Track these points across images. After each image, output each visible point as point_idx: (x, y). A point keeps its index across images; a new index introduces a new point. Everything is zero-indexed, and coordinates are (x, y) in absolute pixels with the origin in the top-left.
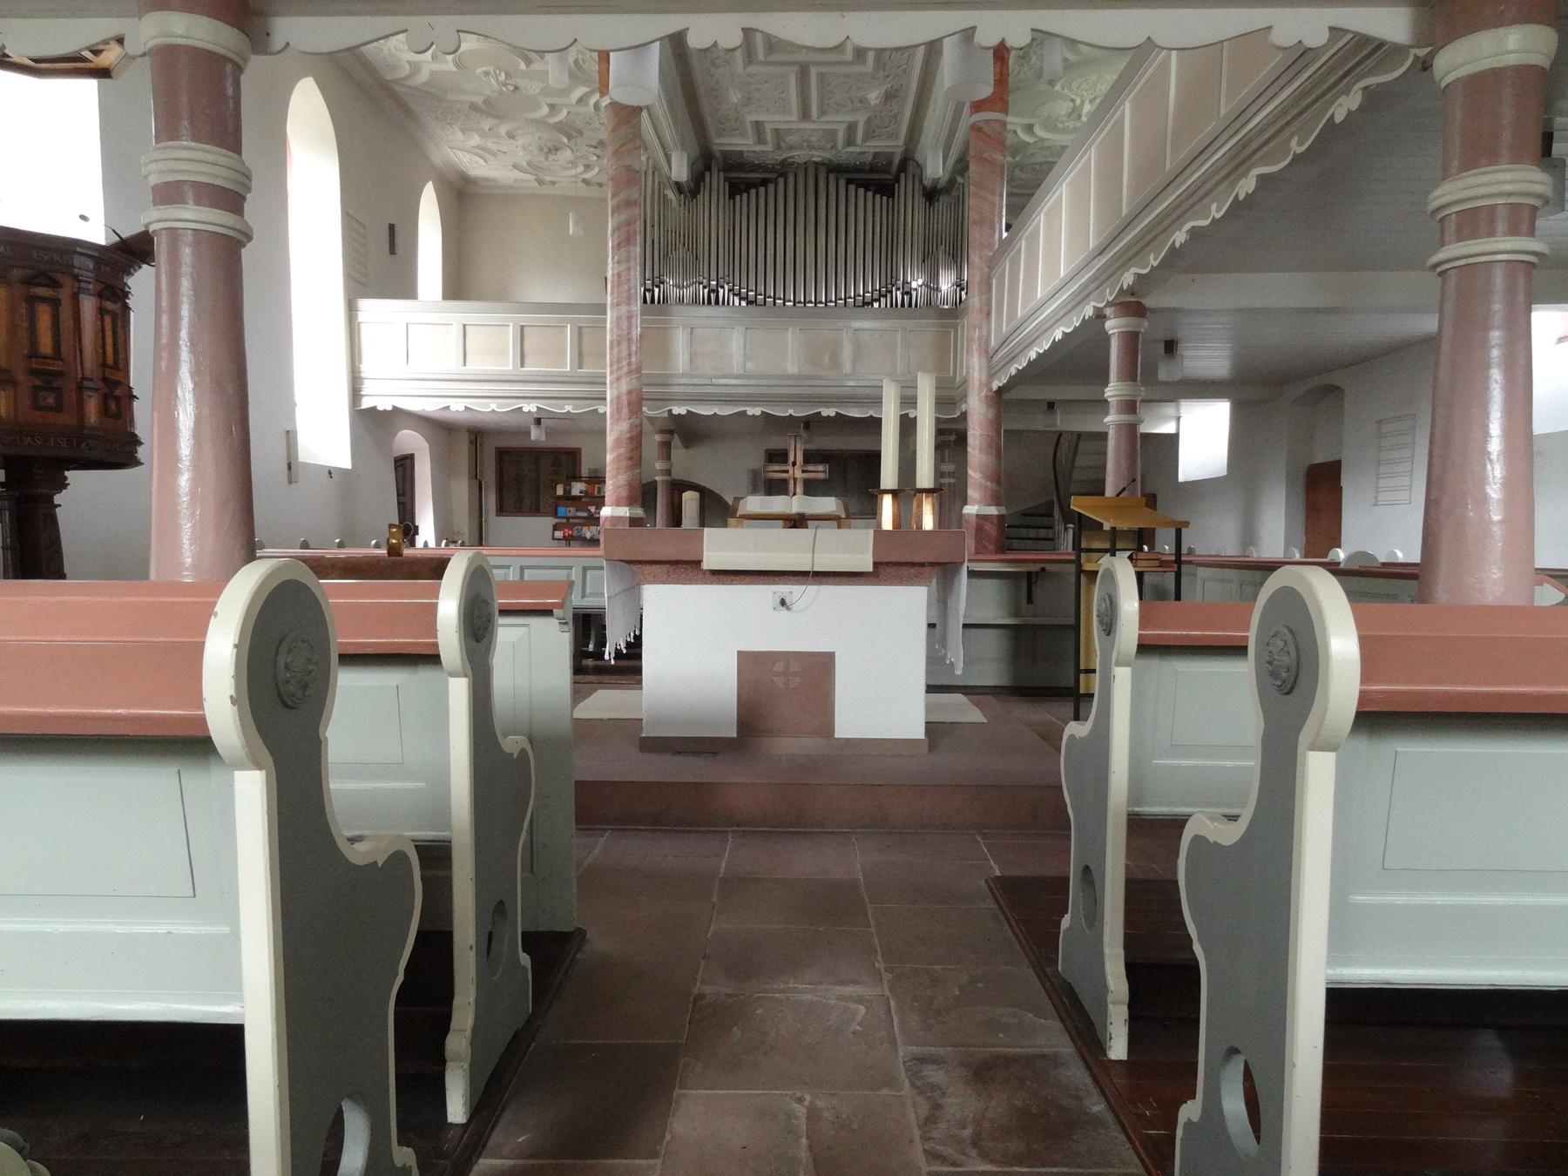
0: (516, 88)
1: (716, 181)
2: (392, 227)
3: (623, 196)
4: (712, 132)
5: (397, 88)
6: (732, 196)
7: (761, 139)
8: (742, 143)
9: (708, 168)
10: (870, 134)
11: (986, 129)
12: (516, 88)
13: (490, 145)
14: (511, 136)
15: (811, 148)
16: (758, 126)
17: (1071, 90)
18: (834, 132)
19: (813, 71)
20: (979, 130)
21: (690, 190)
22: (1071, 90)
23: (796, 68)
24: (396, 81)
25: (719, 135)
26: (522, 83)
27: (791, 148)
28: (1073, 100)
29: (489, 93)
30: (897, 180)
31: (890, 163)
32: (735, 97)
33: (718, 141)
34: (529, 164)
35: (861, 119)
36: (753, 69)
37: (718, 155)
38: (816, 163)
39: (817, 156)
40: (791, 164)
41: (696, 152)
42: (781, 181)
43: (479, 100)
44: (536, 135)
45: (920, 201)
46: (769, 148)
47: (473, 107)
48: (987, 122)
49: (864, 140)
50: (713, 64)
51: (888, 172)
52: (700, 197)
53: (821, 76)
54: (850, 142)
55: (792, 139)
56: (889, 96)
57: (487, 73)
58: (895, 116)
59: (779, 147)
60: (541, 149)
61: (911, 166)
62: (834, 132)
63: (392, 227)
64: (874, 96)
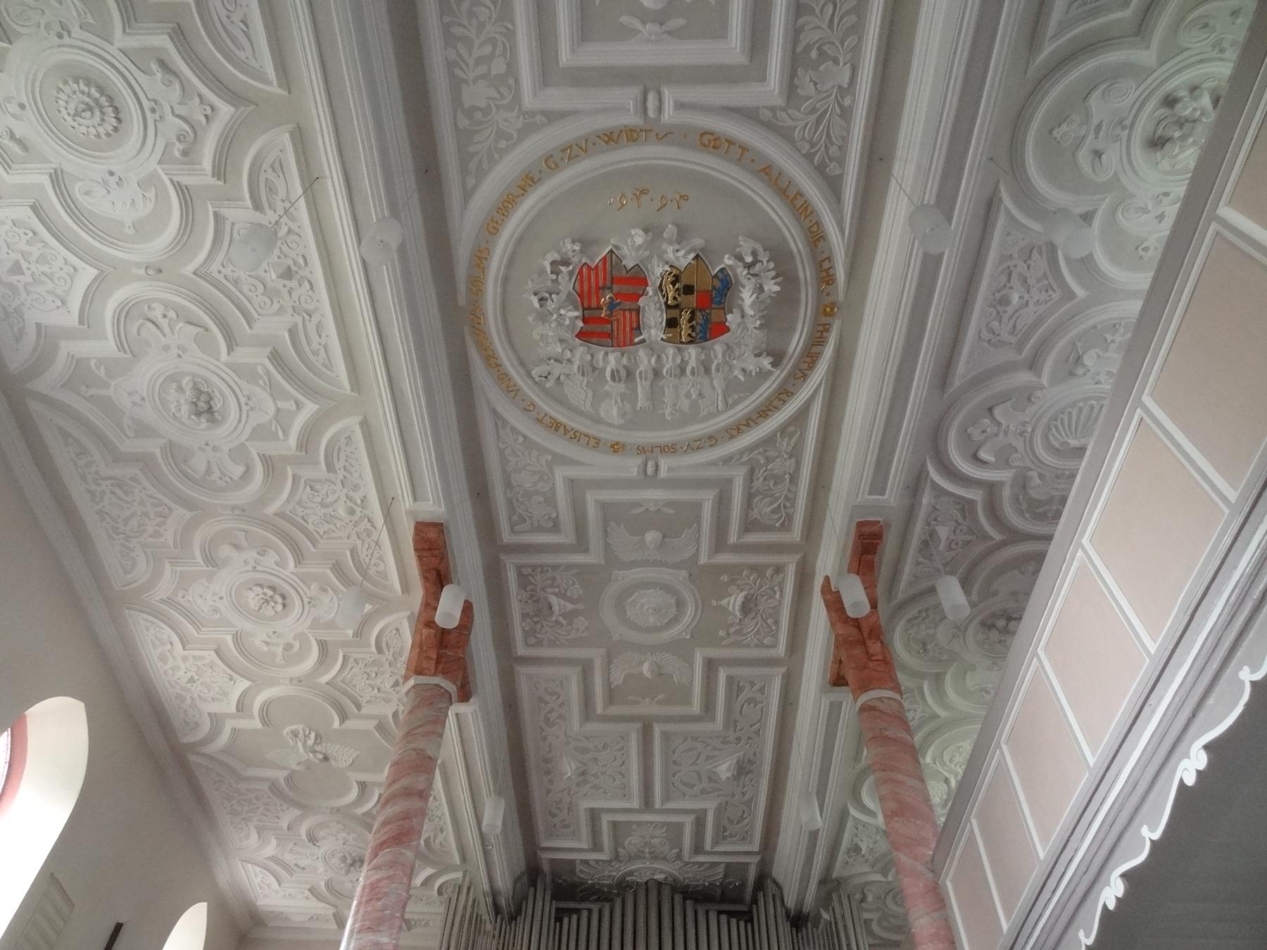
0: (326, 759)
1: (542, 906)
2: (119, 927)
3: (404, 782)
4: (540, 821)
5: (192, 758)
6: (559, 919)
7: (596, 846)
8: (570, 846)
9: (533, 883)
10: (721, 834)
11: (881, 706)
12: (326, 759)
13: (289, 858)
14: (313, 839)
15: (655, 857)
16: (594, 815)
17: (943, 763)
18: (680, 826)
19: (657, 729)
20: (873, 708)
21: (509, 913)
22: (943, 763)
23: (639, 725)
24: (193, 747)
25: (550, 836)
26: (332, 749)
27: (631, 859)
28: (947, 781)
29: (294, 767)
30: (755, 901)
31: (743, 884)
32: (568, 768)
33: (545, 844)
34: (329, 885)
35: (710, 805)
36: (591, 727)
37: (546, 868)
38: (659, 884)
39: (661, 870)
40: (629, 886)
41: (521, 866)
42: (618, 902)
43: (280, 776)
44: (343, 835)
45: (785, 928)
46: (603, 857)
47: (274, 788)
48: (880, 699)
49: (716, 842)
50: (547, 720)
51: (739, 901)
52: (520, 919)
53: (666, 736)
54: (698, 848)
55: (632, 842)
56: (744, 769)
57: (295, 734)
58: (748, 803)
59: (617, 857)
60: (344, 859)
61: (769, 884)
62: (680, 826)
63: (119, 927)
64: (725, 769)
